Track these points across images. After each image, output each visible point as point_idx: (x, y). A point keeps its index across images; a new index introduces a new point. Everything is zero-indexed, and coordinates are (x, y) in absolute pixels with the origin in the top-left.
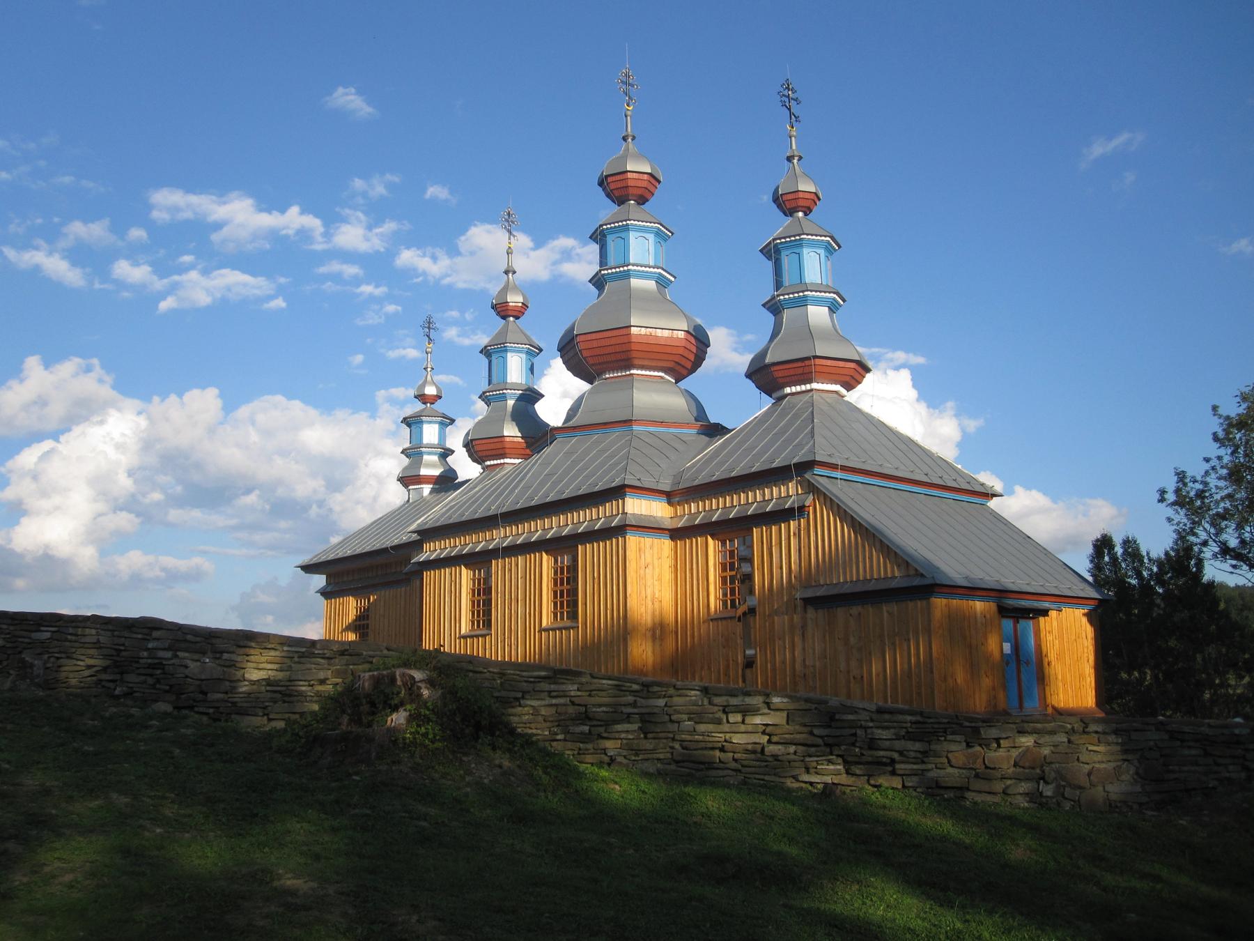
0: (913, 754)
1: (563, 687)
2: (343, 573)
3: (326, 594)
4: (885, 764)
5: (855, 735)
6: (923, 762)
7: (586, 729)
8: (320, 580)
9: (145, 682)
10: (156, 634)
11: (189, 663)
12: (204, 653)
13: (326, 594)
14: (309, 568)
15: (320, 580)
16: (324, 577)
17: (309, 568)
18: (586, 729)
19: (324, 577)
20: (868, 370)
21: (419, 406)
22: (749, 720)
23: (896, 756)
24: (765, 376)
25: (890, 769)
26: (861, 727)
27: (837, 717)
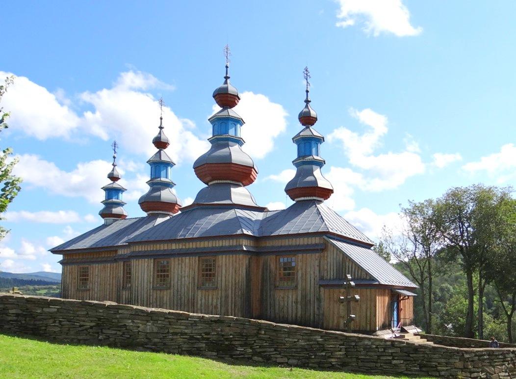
0: (444, 364)
1: (315, 337)
2: (69, 254)
3: (61, 262)
4: (433, 367)
6: (447, 367)
7: (324, 354)
8: (60, 257)
9: (116, 334)
10: (120, 311)
11: (140, 325)
12: (148, 321)
13: (61, 262)
14: (55, 251)
15: (60, 257)
16: (62, 256)
17: (55, 251)
18: (324, 354)
19: (62, 256)
22: (387, 351)
24: (292, 190)
25: (435, 369)
26: (426, 354)
27: (418, 350)
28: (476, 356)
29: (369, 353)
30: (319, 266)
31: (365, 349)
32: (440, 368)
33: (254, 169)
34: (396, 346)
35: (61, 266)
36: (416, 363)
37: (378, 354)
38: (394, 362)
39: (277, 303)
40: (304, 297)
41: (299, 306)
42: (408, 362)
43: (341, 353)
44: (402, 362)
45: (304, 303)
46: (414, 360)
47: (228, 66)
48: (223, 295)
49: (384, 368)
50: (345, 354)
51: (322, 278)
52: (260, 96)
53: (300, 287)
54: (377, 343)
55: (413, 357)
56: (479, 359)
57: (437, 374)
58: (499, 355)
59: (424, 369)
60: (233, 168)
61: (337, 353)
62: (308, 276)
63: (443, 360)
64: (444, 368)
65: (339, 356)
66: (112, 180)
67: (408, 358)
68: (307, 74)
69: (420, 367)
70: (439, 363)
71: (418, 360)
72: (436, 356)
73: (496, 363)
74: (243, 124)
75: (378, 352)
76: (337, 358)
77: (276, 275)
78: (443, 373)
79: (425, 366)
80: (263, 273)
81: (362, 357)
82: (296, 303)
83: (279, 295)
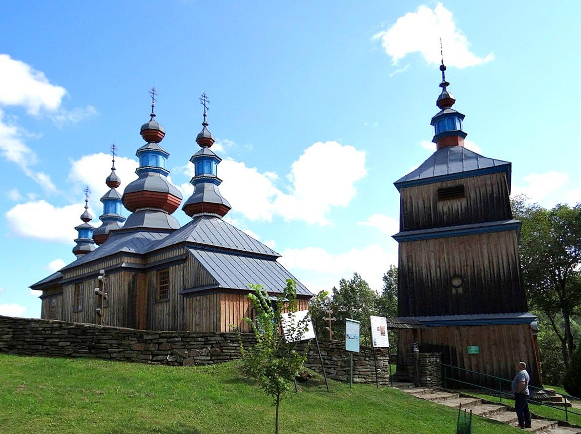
0: (115, 345)
2: (50, 288)
3: (41, 297)
5: (93, 338)
6: (118, 348)
8: (40, 293)
13: (41, 297)
14: (34, 287)
15: (40, 293)
17: (34, 287)
20: (230, 209)
21: (82, 222)
22: (53, 333)
23: (108, 346)
25: (106, 351)
26: (96, 335)
28: (162, 337)
29: (36, 336)
30: (183, 276)
31: (32, 331)
32: (110, 349)
33: (170, 194)
34: (63, 328)
35: (41, 300)
36: (84, 345)
37: (45, 336)
38: (61, 344)
39: (157, 317)
40: (174, 308)
41: (171, 318)
42: (76, 344)
43: (8, 336)
44: (69, 344)
45: (173, 314)
46: (84, 342)
47: (154, 105)
48: (112, 311)
49: (51, 351)
50: (12, 337)
51: (184, 289)
52: (328, 143)
53: (171, 299)
54: (44, 325)
55: (81, 339)
56: (168, 342)
57: (107, 356)
58: (197, 337)
59: (93, 351)
60: (145, 195)
61: (5, 336)
62: (176, 286)
63: (114, 342)
64: (115, 350)
65: (5, 340)
66: (84, 221)
67: (76, 340)
68: (204, 98)
69: (90, 349)
70: (111, 345)
71: (86, 342)
72: (106, 337)
73: (193, 347)
74: (220, 162)
75: (46, 334)
76: (6, 341)
77: (157, 289)
78: (114, 355)
79: (93, 348)
80: (149, 288)
81: (29, 340)
82: (169, 314)
83: (158, 308)
